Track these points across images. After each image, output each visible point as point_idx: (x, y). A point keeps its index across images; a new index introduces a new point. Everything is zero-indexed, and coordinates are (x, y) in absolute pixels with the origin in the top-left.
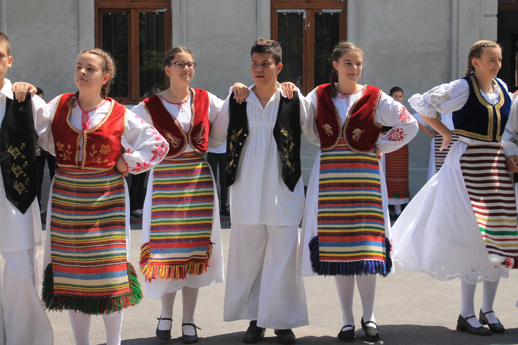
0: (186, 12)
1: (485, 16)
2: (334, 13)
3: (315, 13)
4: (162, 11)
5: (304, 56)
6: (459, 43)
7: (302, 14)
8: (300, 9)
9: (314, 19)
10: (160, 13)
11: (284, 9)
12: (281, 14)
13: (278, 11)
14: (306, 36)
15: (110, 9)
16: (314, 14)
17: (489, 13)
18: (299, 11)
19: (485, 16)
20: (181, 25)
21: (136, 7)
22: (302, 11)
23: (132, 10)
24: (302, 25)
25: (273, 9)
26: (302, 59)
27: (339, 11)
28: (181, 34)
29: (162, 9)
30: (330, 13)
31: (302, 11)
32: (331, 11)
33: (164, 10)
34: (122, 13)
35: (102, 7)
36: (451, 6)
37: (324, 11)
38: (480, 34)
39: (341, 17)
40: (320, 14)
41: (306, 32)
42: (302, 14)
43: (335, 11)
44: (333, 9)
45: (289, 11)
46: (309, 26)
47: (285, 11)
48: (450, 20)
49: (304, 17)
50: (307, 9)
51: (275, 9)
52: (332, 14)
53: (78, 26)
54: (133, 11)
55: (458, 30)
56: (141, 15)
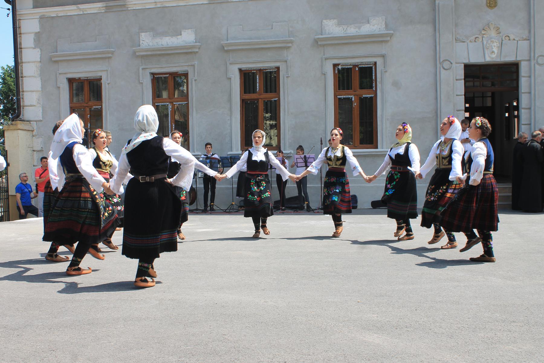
0: (287, 100)
1: (457, 95)
2: (370, 97)
3: (359, 97)
4: (275, 99)
5: (353, 122)
6: (441, 111)
7: (352, 98)
8: (351, 95)
9: (358, 100)
10: (274, 100)
11: (341, 96)
12: (339, 98)
13: (338, 97)
14: (354, 110)
15: (249, 100)
16: (358, 98)
17: (459, 94)
18: (350, 96)
19: (457, 95)
20: (285, 106)
21: (261, 98)
22: (352, 96)
23: (260, 100)
24: (352, 104)
25: (335, 96)
26: (352, 122)
27: (373, 95)
28: (285, 111)
29: (276, 98)
30: (368, 97)
31: (352, 96)
32: (368, 96)
33: (277, 99)
34: (255, 101)
35: (244, 98)
37: (364, 96)
38: (454, 106)
39: (374, 99)
40: (362, 98)
41: (354, 108)
42: (352, 98)
43: (370, 96)
44: (369, 95)
45: (344, 97)
46: (355, 104)
47: (342, 97)
48: (437, 98)
49: (353, 99)
50: (354, 95)
51: (336, 96)
52: (369, 97)
53: (231, 109)
54: (260, 100)
55: (441, 105)
56: (264, 101)
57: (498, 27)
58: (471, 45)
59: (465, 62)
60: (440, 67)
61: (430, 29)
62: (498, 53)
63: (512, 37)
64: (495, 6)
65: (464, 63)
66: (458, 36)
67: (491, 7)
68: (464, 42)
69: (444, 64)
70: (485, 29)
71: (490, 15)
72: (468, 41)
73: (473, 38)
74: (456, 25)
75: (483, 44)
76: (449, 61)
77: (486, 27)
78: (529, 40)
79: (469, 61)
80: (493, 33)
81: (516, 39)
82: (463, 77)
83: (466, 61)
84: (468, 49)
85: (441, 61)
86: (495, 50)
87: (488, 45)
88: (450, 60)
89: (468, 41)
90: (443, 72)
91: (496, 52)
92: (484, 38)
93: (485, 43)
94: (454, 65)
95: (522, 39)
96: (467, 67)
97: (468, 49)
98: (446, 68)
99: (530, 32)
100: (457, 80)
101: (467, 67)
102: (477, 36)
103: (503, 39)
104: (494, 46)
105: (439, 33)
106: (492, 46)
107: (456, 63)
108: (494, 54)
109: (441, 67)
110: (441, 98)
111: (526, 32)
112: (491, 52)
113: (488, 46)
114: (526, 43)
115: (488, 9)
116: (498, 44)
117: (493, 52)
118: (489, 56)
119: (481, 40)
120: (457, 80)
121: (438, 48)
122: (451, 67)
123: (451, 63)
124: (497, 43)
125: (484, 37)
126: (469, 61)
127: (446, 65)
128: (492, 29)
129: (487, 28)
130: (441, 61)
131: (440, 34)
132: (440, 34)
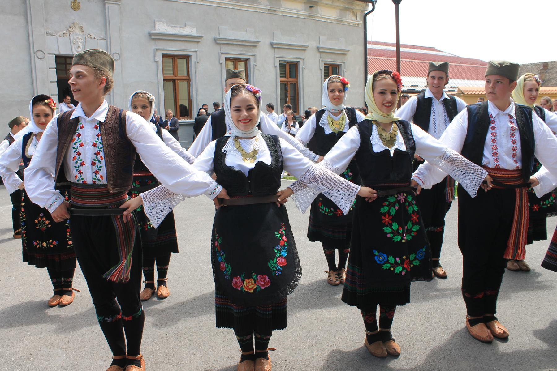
1: (51, 82)
19: (51, 82)
36: (32, 77)
48: (32, 84)
57: (81, 26)
58: (60, 39)
59: (56, 53)
60: (35, 56)
61: (22, 20)
62: (82, 48)
63: (93, 36)
64: (79, 9)
65: (54, 54)
66: (48, 30)
67: (76, 9)
68: (54, 36)
69: (38, 54)
70: (71, 27)
71: (74, 16)
72: (57, 36)
73: (61, 33)
74: (46, 21)
75: (70, 39)
76: (42, 51)
77: (72, 26)
78: (105, 40)
79: (59, 53)
80: (78, 31)
81: (97, 38)
82: (55, 67)
83: (57, 53)
84: (58, 42)
85: (35, 51)
86: (80, 45)
87: (74, 41)
88: (43, 51)
89: (57, 36)
90: (37, 60)
91: (81, 47)
92: (70, 35)
93: (72, 38)
94: (47, 55)
95: (100, 38)
96: (58, 57)
97: (58, 42)
98: (40, 57)
99: (106, 33)
100: (50, 68)
101: (58, 57)
102: (64, 32)
103: (86, 37)
104: (80, 42)
105: (32, 25)
106: (78, 42)
107: (49, 54)
108: (80, 48)
109: (36, 58)
110: (38, 84)
111: (103, 33)
112: (78, 46)
113: (74, 41)
114: (104, 42)
115: (72, 10)
116: (82, 40)
117: (79, 47)
118: (76, 50)
119: (68, 36)
120: (50, 68)
121: (31, 39)
122: (45, 57)
123: (44, 54)
124: (81, 39)
125: (71, 34)
126: (59, 53)
127: (40, 54)
128: (77, 27)
129: (72, 26)
130: (35, 51)
131: (32, 27)
132: (32, 27)
